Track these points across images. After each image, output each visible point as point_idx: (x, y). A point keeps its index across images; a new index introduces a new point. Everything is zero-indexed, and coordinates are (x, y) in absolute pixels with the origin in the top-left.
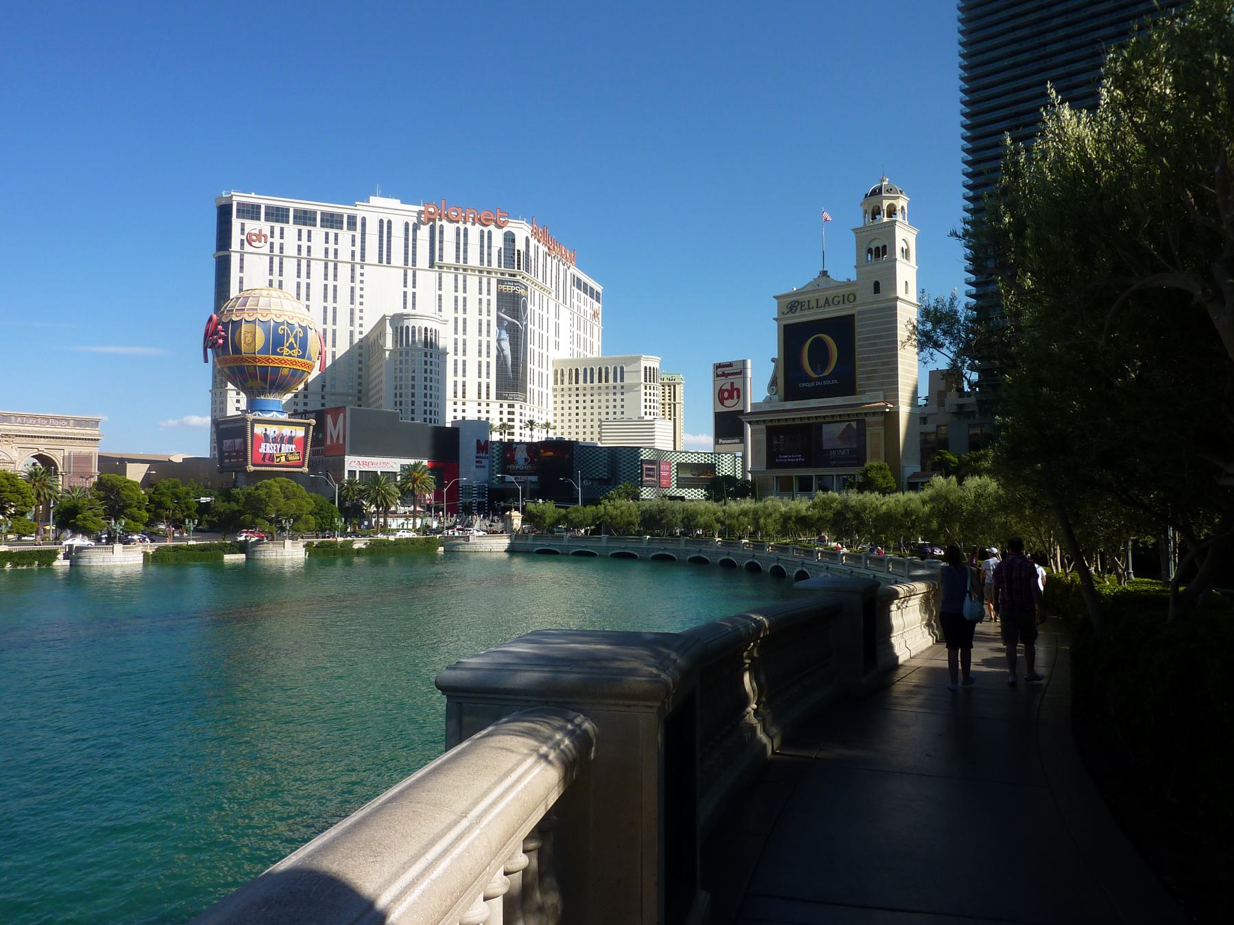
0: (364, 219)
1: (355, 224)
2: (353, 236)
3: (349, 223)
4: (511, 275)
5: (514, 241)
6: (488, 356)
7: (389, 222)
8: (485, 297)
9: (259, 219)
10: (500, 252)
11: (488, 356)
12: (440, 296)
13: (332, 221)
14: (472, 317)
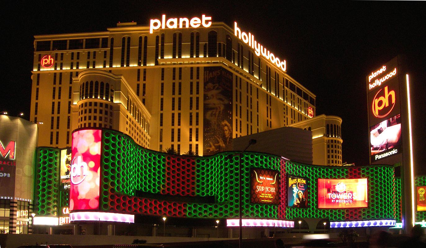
0: (112, 39)
1: (107, 43)
2: (105, 52)
3: (103, 43)
4: (214, 63)
5: (215, 37)
6: (197, 124)
7: (129, 38)
8: (195, 81)
9: (49, 50)
10: (205, 46)
11: (197, 124)
12: (162, 84)
13: (92, 43)
14: (186, 96)
